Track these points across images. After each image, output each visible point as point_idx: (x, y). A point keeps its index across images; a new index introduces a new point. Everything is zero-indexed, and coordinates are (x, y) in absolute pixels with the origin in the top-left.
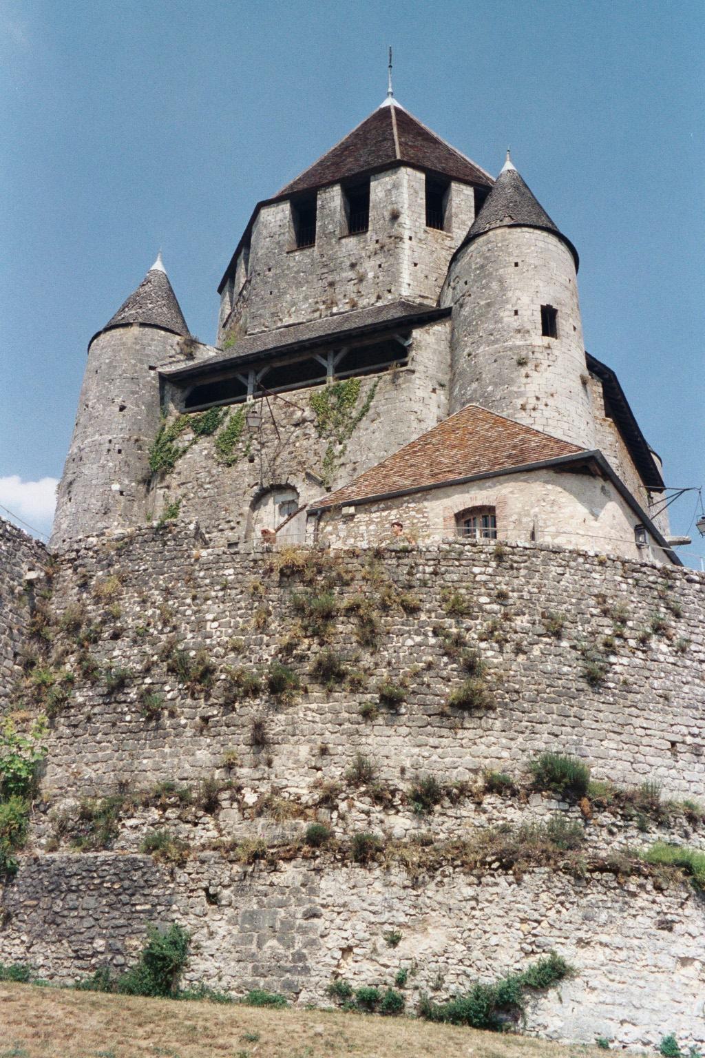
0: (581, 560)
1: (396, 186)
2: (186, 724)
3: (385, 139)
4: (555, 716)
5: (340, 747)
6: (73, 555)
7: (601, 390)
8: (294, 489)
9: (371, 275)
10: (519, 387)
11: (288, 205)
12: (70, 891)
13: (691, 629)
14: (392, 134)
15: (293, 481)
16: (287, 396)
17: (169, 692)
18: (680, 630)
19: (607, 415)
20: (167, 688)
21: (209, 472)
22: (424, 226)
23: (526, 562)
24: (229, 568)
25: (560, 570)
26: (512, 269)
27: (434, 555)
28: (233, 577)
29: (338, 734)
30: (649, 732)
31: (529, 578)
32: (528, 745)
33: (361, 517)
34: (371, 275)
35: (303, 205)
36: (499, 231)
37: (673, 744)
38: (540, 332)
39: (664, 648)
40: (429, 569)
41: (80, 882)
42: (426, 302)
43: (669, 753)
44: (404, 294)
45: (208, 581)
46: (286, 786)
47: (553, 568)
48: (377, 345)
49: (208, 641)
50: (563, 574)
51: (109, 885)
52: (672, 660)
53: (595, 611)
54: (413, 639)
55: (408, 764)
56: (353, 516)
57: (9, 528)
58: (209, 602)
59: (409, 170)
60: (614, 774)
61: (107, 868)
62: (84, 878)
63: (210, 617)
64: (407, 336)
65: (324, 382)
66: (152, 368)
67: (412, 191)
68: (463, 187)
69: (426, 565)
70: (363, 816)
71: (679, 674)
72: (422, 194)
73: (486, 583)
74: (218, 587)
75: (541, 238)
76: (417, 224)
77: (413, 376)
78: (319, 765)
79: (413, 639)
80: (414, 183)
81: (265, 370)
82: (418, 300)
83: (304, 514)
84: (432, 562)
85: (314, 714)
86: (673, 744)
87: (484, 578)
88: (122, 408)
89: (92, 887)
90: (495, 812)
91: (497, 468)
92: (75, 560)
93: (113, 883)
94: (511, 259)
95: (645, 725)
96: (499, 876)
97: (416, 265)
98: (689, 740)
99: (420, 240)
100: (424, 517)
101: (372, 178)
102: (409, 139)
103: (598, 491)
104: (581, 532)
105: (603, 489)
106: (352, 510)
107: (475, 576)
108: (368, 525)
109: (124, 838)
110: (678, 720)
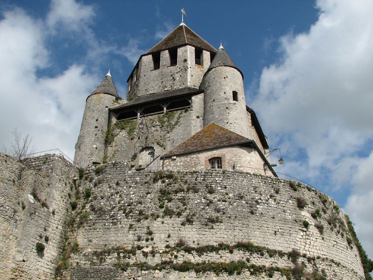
0: (249, 176)
2: (125, 227)
4: (241, 225)
5: (174, 235)
7: (250, 117)
8: (153, 148)
9: (178, 79)
10: (226, 116)
11: (151, 55)
12: (91, 277)
14: (184, 34)
15: (152, 145)
17: (119, 216)
18: (278, 197)
19: (252, 125)
20: (119, 215)
21: (125, 142)
22: (195, 64)
23: (232, 176)
24: (137, 177)
25: (242, 179)
26: (223, 79)
27: (203, 174)
28: (139, 180)
29: (174, 231)
30: (268, 228)
31: (233, 181)
32: (233, 234)
33: (178, 159)
34: (178, 79)
36: (219, 67)
37: (275, 232)
39: (273, 203)
40: (202, 179)
41: (94, 275)
42: (195, 87)
43: (274, 235)
44: (189, 85)
46: (158, 247)
48: (180, 101)
49: (131, 201)
51: (103, 276)
52: (275, 206)
53: (253, 192)
54: (197, 201)
55: (196, 240)
57: (68, 163)
58: (131, 188)
59: (190, 46)
60: (258, 242)
61: (102, 271)
62: (96, 274)
63: (132, 193)
64: (190, 99)
65: (163, 113)
66: (106, 107)
67: (191, 53)
68: (207, 52)
69: (201, 177)
70: (182, 256)
71: (277, 211)
72: (194, 54)
73: (219, 183)
74: (134, 184)
78: (168, 240)
79: (197, 201)
82: (193, 87)
83: (159, 158)
84: (202, 176)
85: (166, 224)
86: (275, 232)
87: (219, 181)
88: (97, 120)
89: (98, 277)
90: (223, 254)
91: (222, 145)
93: (105, 275)
94: (223, 76)
95: (267, 227)
96: (224, 274)
97: (192, 76)
98: (280, 230)
99: (194, 68)
100: (198, 160)
102: (189, 36)
104: (248, 166)
106: (175, 157)
107: (217, 181)
108: (180, 163)
109: (107, 262)
110: (277, 225)
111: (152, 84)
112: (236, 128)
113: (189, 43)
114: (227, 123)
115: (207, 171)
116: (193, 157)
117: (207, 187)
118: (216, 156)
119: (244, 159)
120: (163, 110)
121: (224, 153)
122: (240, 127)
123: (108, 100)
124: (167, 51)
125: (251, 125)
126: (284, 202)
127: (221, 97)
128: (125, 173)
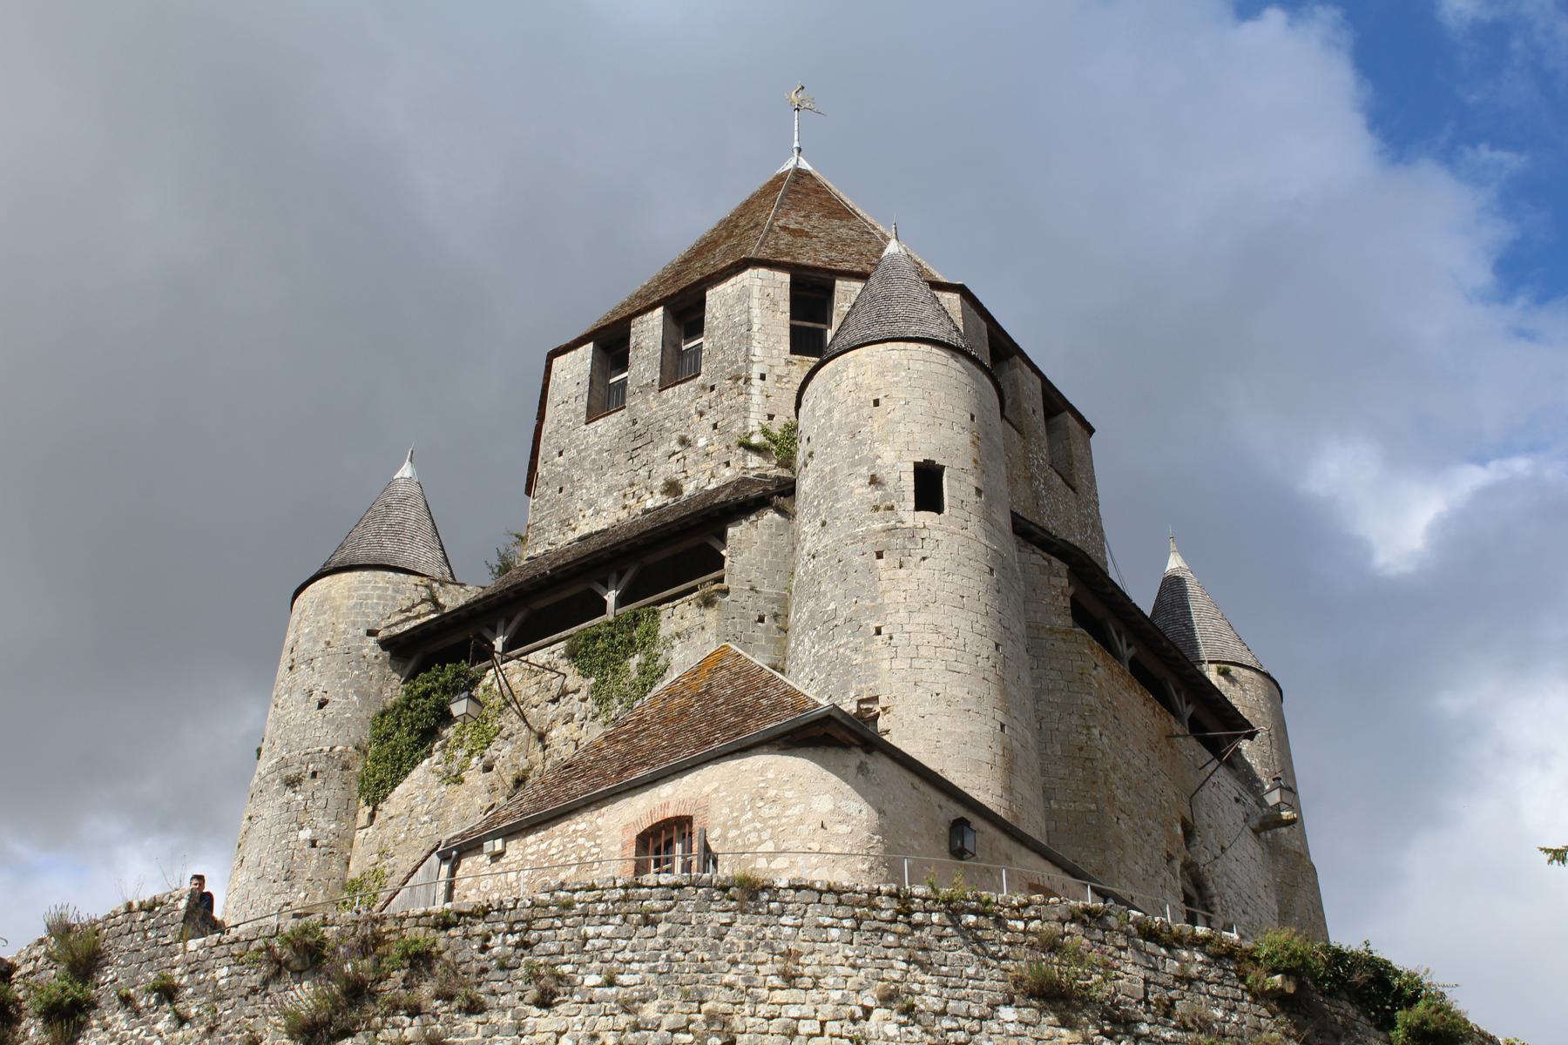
1: (744, 295)
6: (30, 967)
7: (1065, 582)
9: (702, 442)
10: (874, 599)
13: (946, 993)
16: (540, 657)
22: (787, 355)
23: (669, 909)
34: (702, 442)
35: (611, 344)
38: (912, 505)
45: (190, 991)
47: (715, 916)
50: (730, 925)
56: (501, 854)
59: (762, 271)
64: (722, 538)
66: (371, 633)
67: (767, 303)
72: (786, 306)
73: (602, 950)
76: (775, 352)
77: (727, 599)
80: (770, 290)
81: (519, 618)
84: (517, 927)
87: (599, 943)
88: (322, 704)
92: (32, 973)
97: (771, 417)
99: (780, 378)
100: (596, 845)
103: (852, 770)
105: (862, 768)
106: (499, 844)
107: (586, 939)
111: (592, 487)
112: (923, 651)
113: (765, 253)
114: (878, 632)
115: (545, 897)
116: (575, 831)
117: (533, 976)
118: (670, 814)
119: (796, 811)
120: (601, 608)
121: (707, 789)
123: (380, 598)
124: (659, 311)
125: (1064, 621)
126: (967, 1024)
128: (173, 955)
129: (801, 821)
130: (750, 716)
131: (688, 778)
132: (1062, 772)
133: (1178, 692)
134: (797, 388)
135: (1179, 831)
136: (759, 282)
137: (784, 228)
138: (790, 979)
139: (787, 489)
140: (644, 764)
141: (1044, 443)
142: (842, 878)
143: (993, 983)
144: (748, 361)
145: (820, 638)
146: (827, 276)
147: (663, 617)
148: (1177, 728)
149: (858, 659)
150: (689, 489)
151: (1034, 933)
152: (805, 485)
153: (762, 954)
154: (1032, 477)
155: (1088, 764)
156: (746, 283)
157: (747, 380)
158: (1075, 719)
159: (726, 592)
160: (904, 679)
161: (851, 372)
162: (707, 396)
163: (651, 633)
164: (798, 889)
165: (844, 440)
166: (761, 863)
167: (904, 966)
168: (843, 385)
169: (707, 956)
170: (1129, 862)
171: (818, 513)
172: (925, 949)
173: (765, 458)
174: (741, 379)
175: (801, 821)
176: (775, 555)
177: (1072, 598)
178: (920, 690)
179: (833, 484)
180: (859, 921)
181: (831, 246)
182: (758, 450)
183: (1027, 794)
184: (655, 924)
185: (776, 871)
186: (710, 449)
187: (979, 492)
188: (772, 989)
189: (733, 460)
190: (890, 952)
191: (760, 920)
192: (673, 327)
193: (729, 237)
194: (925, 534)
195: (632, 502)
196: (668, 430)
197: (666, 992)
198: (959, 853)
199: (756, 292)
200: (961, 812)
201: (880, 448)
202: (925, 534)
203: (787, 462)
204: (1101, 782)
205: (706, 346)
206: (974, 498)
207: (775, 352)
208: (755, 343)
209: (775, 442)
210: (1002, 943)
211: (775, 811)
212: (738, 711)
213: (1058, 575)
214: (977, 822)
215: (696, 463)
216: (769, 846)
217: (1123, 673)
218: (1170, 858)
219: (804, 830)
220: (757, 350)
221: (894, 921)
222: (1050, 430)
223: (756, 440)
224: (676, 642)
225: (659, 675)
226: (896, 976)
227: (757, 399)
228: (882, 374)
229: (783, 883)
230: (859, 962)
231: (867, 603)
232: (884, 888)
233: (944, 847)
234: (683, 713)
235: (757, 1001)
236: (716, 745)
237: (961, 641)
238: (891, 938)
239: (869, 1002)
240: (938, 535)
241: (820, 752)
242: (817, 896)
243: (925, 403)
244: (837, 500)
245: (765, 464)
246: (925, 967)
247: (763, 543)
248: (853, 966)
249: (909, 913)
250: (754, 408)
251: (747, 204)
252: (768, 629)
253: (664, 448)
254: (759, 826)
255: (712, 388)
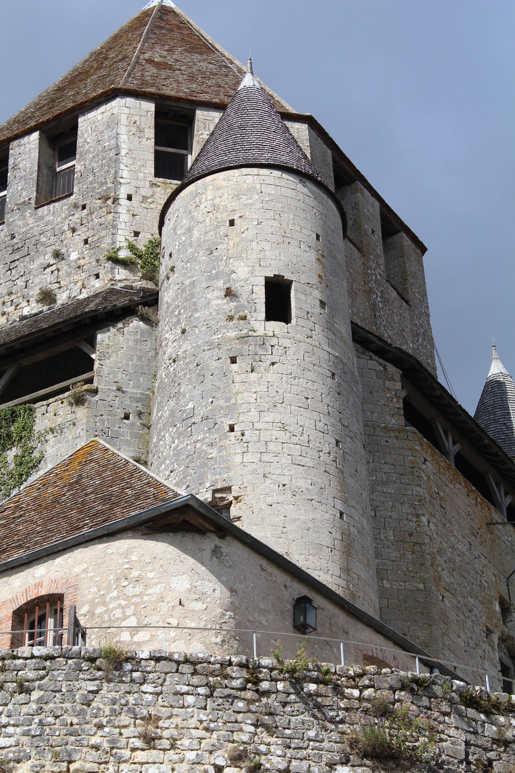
1: (113, 123)
3: (124, 58)
7: (399, 385)
9: (74, 256)
10: (228, 400)
13: (289, 753)
22: (151, 177)
23: (42, 678)
25: (92, 686)
34: (74, 256)
38: (263, 315)
47: (84, 684)
50: (96, 692)
59: (130, 101)
64: (92, 343)
67: (134, 130)
72: (151, 133)
75: (271, 180)
76: (141, 175)
77: (97, 398)
80: (136, 118)
97: (137, 234)
99: (145, 198)
101: (81, 120)
103: (208, 553)
105: (216, 551)
112: (272, 447)
113: (133, 85)
114: (232, 429)
118: (43, 592)
121: (77, 570)
122: (295, 440)
124: (36, 135)
125: (397, 421)
127: (211, 313)
129: (162, 599)
130: (117, 504)
131: (60, 560)
132: (394, 555)
133: (497, 484)
134: (160, 207)
135: (497, 608)
136: (126, 111)
137: (150, 61)
138: (150, 741)
139: (151, 299)
140: (20, 547)
141: (382, 261)
142: (197, 649)
143: (331, 745)
144: (116, 183)
145: (179, 434)
146: (188, 106)
147: (38, 413)
148: (497, 517)
149: (214, 453)
150: (62, 298)
151: (368, 700)
152: (167, 297)
153: (125, 719)
154: (371, 291)
155: (417, 548)
156: (115, 111)
157: (116, 200)
158: (406, 508)
159: (95, 392)
160: (254, 472)
161: (210, 194)
162: (79, 214)
163: (28, 428)
164: (158, 660)
165: (203, 257)
166: (125, 636)
167: (252, 729)
168: (202, 206)
169: (75, 720)
170: (453, 636)
171: (178, 322)
172: (271, 714)
173: (131, 271)
174: (110, 199)
175: (162, 599)
176: (140, 358)
177: (405, 401)
178: (268, 481)
179: (192, 295)
180: (212, 688)
181: (192, 78)
182: (125, 263)
183: (363, 575)
184: (29, 691)
185: (139, 644)
186: (82, 262)
187: (323, 304)
188: (133, 750)
189: (102, 272)
190: (240, 717)
191: (124, 687)
192: (48, 151)
193: (99, 68)
194: (274, 341)
195: (10, 309)
196: (43, 244)
197: (38, 753)
198: (302, 628)
199: (124, 120)
200: (304, 591)
201: (235, 264)
202: (274, 341)
203: (151, 275)
204: (428, 564)
205: (78, 168)
206: (318, 310)
207: (141, 175)
208: (122, 167)
209: (140, 257)
210: (340, 709)
211: (138, 590)
212: (105, 500)
213: (392, 379)
214: (318, 600)
215: (69, 275)
216: (132, 622)
217: (449, 467)
218: (489, 632)
219: (164, 607)
220: (125, 173)
221: (244, 689)
222: (387, 248)
223: (123, 254)
224: (50, 436)
225: (35, 467)
226: (245, 738)
227: (124, 217)
228: (237, 197)
229: (145, 655)
230: (212, 725)
231: (222, 403)
232: (235, 659)
233: (289, 623)
234: (56, 501)
235: (120, 761)
236: (85, 530)
237: (305, 438)
238: (240, 705)
239: (221, 762)
240: (286, 343)
241: (179, 537)
242: (175, 666)
243: (276, 224)
244: (196, 310)
245: (131, 277)
246: (270, 730)
247: (129, 348)
248: (207, 729)
249: (257, 682)
250: (121, 226)
251: (116, 38)
252: (132, 425)
253: (40, 261)
254: (123, 603)
255: (84, 207)
